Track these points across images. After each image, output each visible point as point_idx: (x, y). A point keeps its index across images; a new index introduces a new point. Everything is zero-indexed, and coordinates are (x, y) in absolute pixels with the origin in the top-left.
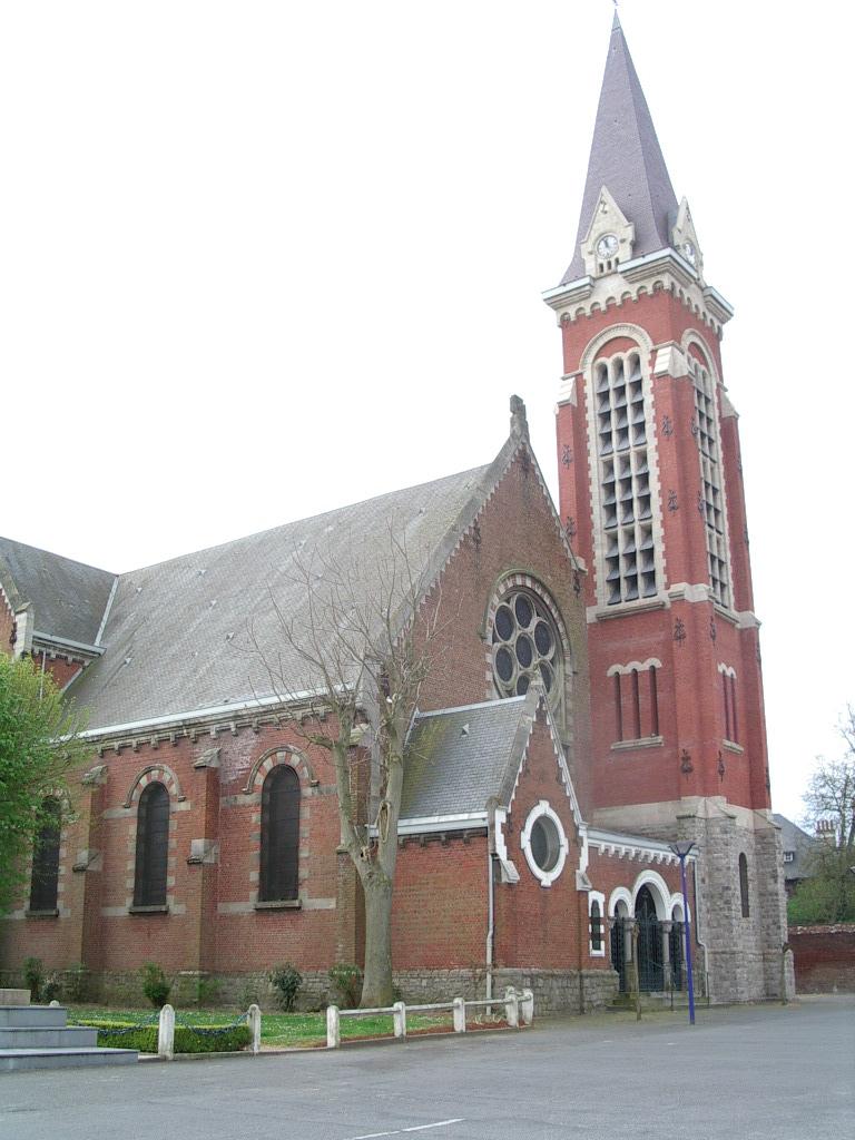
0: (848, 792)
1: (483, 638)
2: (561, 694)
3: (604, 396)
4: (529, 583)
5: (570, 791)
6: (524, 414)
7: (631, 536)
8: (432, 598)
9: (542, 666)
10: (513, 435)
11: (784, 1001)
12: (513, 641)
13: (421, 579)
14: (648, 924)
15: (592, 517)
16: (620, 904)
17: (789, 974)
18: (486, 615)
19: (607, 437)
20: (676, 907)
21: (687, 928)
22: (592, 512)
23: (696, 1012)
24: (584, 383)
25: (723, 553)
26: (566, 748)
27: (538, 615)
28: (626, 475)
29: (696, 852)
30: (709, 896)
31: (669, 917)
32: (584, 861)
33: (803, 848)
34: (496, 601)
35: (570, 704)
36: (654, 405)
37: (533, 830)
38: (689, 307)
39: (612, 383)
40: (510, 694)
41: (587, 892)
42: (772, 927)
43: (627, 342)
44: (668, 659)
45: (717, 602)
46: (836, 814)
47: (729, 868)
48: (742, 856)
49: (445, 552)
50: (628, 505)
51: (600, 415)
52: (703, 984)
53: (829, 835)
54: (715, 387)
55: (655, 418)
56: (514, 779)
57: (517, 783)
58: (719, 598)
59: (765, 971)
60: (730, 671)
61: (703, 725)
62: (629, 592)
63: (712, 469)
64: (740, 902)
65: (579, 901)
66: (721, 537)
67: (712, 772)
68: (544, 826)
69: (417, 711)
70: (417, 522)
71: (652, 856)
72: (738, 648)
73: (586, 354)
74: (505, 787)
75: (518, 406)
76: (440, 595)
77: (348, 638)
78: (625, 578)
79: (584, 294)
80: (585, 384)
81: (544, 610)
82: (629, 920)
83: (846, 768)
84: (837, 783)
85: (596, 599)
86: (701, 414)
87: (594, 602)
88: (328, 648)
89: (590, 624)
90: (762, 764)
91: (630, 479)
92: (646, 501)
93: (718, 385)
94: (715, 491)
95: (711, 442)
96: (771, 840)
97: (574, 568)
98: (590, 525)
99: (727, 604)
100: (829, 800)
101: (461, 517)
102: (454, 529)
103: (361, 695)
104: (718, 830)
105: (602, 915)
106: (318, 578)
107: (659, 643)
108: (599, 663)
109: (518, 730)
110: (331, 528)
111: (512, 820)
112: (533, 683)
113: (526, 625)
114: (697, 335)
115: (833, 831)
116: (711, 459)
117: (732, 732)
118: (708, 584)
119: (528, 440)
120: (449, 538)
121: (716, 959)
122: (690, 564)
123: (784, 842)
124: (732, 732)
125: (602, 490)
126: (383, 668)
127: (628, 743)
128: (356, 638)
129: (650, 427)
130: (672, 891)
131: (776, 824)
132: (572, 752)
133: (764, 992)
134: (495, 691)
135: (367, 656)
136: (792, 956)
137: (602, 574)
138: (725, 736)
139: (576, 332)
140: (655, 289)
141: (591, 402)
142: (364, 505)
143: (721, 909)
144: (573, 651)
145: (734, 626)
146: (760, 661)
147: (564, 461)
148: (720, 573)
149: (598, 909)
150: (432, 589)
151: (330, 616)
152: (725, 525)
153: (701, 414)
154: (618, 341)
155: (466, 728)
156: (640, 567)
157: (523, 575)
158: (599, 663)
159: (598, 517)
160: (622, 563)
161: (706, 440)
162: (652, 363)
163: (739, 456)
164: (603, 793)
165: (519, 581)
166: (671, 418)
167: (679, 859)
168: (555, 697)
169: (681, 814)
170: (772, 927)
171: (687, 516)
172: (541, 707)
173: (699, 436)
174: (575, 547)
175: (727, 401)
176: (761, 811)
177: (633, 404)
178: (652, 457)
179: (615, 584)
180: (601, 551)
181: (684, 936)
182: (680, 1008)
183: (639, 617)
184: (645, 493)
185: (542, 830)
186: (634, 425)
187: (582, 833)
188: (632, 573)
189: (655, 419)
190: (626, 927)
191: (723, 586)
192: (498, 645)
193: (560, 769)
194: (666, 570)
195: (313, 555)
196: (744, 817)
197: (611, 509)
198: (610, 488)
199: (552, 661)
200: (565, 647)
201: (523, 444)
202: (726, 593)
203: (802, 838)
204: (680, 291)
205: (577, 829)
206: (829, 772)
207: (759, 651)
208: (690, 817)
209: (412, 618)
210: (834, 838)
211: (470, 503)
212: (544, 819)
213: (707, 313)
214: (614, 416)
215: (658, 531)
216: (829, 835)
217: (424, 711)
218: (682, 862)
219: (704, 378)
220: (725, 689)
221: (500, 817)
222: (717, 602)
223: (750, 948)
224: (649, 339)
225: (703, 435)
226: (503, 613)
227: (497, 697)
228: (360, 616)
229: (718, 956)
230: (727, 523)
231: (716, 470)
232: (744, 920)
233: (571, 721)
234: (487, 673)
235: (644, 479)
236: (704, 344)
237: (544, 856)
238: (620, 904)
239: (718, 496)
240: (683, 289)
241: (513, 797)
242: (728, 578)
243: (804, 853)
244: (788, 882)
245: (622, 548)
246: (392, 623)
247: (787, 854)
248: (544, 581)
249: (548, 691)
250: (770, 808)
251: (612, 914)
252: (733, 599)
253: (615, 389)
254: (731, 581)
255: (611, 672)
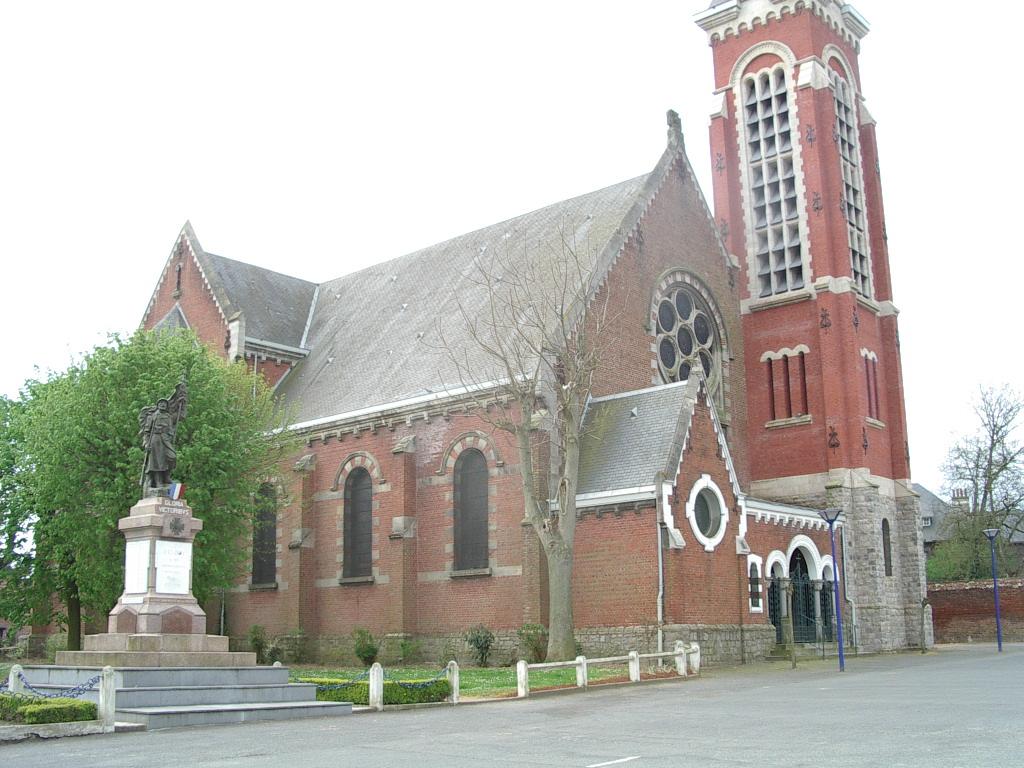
0: (980, 463)
1: (648, 330)
2: (719, 378)
3: (752, 108)
4: (688, 280)
5: (729, 465)
6: (683, 139)
7: (779, 235)
8: (601, 294)
9: (701, 354)
10: (670, 146)
11: (924, 650)
12: (674, 332)
13: (591, 277)
14: (801, 583)
15: (744, 218)
16: (776, 566)
17: (928, 626)
18: (649, 310)
19: (756, 146)
20: (826, 568)
21: (836, 586)
22: (744, 214)
23: (845, 661)
24: (734, 97)
25: (863, 248)
26: (724, 427)
27: (697, 308)
28: (774, 180)
29: (843, 518)
30: (856, 558)
31: (820, 577)
32: (743, 528)
33: (940, 514)
34: (659, 297)
35: (728, 388)
36: (798, 115)
37: (696, 501)
38: (828, 24)
39: (759, 97)
40: (673, 379)
41: (746, 556)
42: (912, 584)
43: (772, 58)
44: (816, 346)
45: (859, 293)
46: (970, 483)
47: (873, 532)
48: (885, 522)
49: (611, 254)
50: (776, 207)
51: (749, 125)
52: (851, 636)
53: (963, 502)
54: (854, 97)
55: (799, 127)
56: (679, 456)
57: (681, 460)
58: (860, 289)
59: (907, 623)
60: (872, 355)
61: (848, 405)
62: (779, 286)
63: (852, 172)
64: (883, 563)
65: (739, 564)
66: (862, 234)
67: (857, 446)
68: (706, 497)
69: (590, 397)
70: (584, 229)
71: (804, 522)
72: (878, 334)
73: (735, 70)
74: (671, 462)
75: (674, 120)
76: (608, 291)
77: (527, 333)
78: (775, 273)
79: (731, 15)
80: (735, 98)
81: (702, 304)
82: (784, 580)
83: (978, 441)
84: (970, 456)
85: (749, 292)
86: (841, 123)
87: (747, 295)
88: (509, 342)
89: (745, 315)
90: (902, 438)
91: (777, 183)
92: (792, 203)
93: (857, 95)
94: (855, 192)
95: (851, 147)
96: (911, 507)
97: (728, 264)
98: (743, 226)
99: (867, 294)
100: (963, 470)
101: (625, 221)
102: (619, 232)
103: (539, 383)
104: (863, 498)
105: (760, 576)
106: (498, 280)
107: (806, 331)
108: (752, 349)
109: (682, 412)
110: (508, 235)
111: (678, 492)
112: (694, 369)
113: (686, 317)
114: (836, 49)
115: (967, 498)
116: (852, 164)
117: (874, 410)
118: (851, 277)
119: (684, 150)
120: (615, 241)
121: (862, 613)
122: (833, 258)
123: (923, 509)
124: (874, 410)
125: (752, 194)
126: (559, 359)
127: (780, 422)
128: (534, 332)
129: (795, 136)
130: (822, 555)
131: (915, 492)
132: (730, 430)
133: (906, 642)
134: (660, 378)
135: (544, 349)
136: (930, 610)
137: (754, 270)
138: (868, 414)
139: (725, 50)
140: (797, 9)
141: (741, 115)
142: (537, 213)
143: (866, 569)
144: (729, 339)
145: (874, 314)
146: (898, 346)
147: (717, 168)
148: (861, 266)
149: (756, 571)
150: (600, 287)
151: (510, 314)
152: (864, 223)
153: (841, 123)
154: (765, 57)
155: (635, 411)
156: (788, 263)
157: (683, 272)
158: (752, 349)
159: (749, 218)
160: (772, 259)
161: (847, 146)
162: (795, 77)
163: (877, 160)
164: (760, 466)
165: (679, 278)
166: (814, 127)
167: (828, 525)
168: (714, 382)
169: (829, 484)
170: (912, 584)
171: (830, 215)
172: (701, 391)
173: (840, 142)
174: (729, 246)
175: (865, 109)
176: (901, 481)
177: (779, 115)
178: (798, 163)
179: (766, 279)
180: (753, 249)
181: (834, 594)
182: (831, 658)
183: (789, 308)
184: (792, 195)
185: (705, 501)
186: (781, 134)
187: (741, 503)
188: (781, 268)
189: (799, 128)
190: (782, 586)
191: (864, 278)
192: (661, 336)
193: (720, 446)
194: (812, 265)
195: (493, 259)
196: (886, 486)
197: (761, 211)
198: (759, 192)
199: (711, 349)
200: (722, 337)
201: (679, 153)
202: (867, 284)
203: (939, 504)
204: (821, 10)
205: (736, 499)
206: (963, 445)
207: (897, 337)
208: (837, 487)
209: (583, 314)
210: (968, 504)
211: (633, 208)
212: (707, 490)
213: (845, 29)
214: (761, 126)
215: (804, 230)
216: (963, 502)
217: (597, 396)
218: (831, 527)
219: (843, 89)
220: (867, 371)
221: (667, 490)
222: (859, 293)
223: (893, 603)
224: (792, 54)
225: (843, 141)
226: (665, 306)
227: (662, 382)
228: (536, 312)
229: (864, 611)
230: (866, 222)
231: (856, 173)
232: (887, 578)
233: (728, 401)
234: (653, 361)
235: (790, 182)
236: (844, 59)
237: (707, 522)
238: (776, 566)
239: (858, 197)
240: (823, 8)
241: (678, 472)
242: (868, 271)
243: (940, 517)
244: (926, 544)
245: (771, 246)
246: (565, 318)
247: (925, 519)
248: (702, 278)
249: (708, 376)
250: (910, 478)
251: (769, 574)
252: (873, 291)
253: (762, 102)
254: (871, 274)
255: (764, 358)
